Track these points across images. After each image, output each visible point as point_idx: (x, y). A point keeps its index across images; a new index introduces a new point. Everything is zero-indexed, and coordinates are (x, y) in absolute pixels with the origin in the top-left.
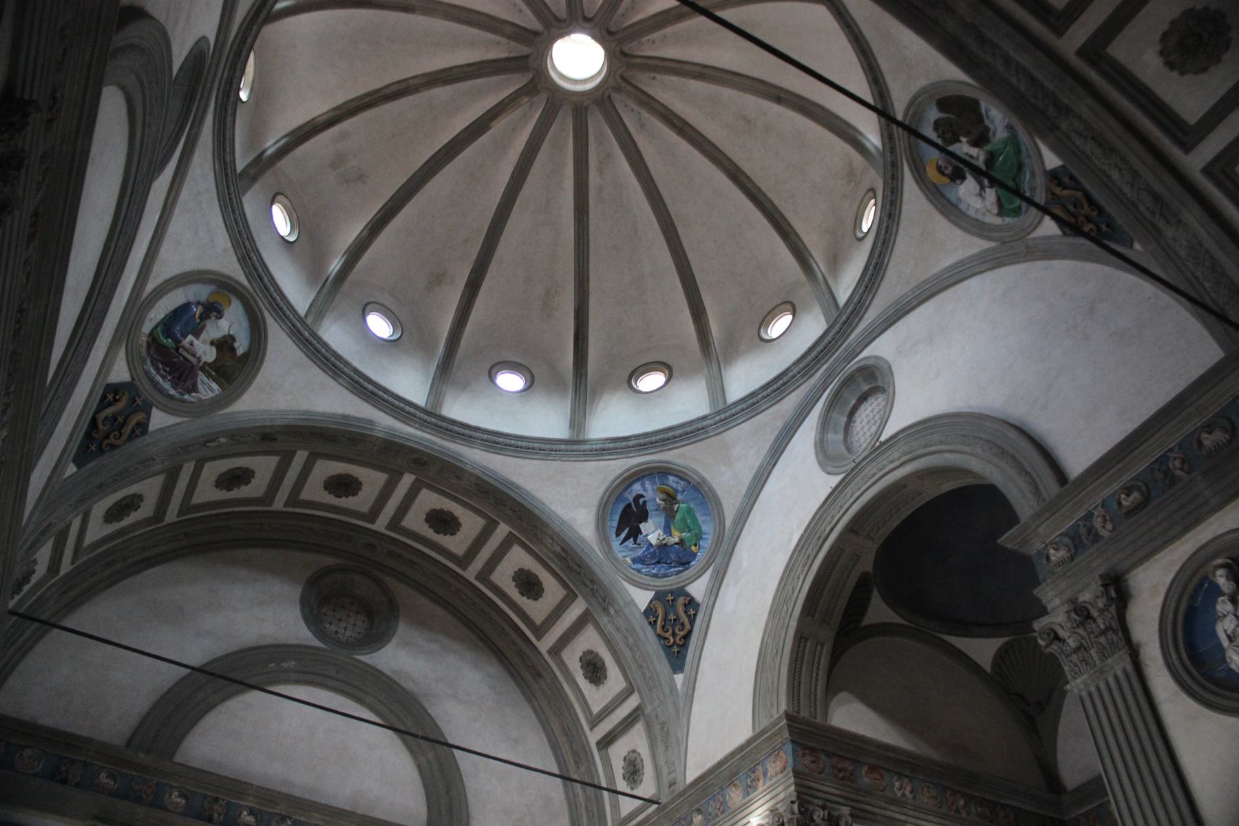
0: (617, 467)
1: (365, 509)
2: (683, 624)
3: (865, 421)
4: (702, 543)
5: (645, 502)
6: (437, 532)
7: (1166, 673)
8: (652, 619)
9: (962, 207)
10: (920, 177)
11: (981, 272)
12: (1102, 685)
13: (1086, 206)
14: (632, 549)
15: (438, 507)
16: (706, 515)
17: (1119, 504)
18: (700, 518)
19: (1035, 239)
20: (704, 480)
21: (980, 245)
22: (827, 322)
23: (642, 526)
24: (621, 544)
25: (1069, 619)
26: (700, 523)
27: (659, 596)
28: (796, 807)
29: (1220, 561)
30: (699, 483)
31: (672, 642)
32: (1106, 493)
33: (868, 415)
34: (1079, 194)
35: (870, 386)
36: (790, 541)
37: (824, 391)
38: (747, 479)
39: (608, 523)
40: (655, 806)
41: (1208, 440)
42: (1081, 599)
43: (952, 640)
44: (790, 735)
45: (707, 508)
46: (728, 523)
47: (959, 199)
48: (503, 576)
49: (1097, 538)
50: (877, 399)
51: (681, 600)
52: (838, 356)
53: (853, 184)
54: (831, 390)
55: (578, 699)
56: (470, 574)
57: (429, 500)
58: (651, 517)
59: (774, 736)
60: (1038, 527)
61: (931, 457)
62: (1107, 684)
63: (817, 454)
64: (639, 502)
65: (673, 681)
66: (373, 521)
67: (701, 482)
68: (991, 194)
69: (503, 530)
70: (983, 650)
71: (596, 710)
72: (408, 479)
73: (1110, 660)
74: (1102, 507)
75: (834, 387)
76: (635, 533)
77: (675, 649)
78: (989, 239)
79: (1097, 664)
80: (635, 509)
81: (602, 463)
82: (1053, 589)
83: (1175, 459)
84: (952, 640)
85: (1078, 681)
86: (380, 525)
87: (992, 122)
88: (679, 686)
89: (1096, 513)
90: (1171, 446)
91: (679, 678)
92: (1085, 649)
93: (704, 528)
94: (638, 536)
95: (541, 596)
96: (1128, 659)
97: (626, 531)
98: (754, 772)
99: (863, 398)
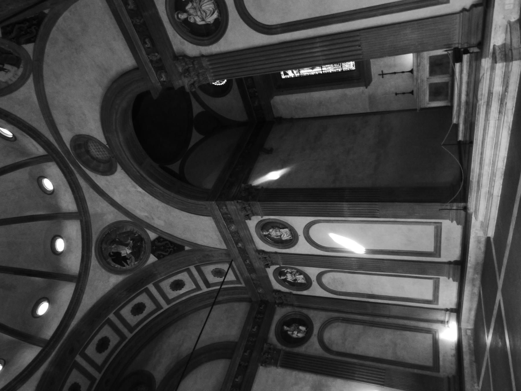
0: (94, 262)
1: (88, 382)
2: (166, 244)
3: (97, 153)
4: (135, 232)
5: (113, 252)
6: (107, 348)
7: (211, 46)
8: (162, 256)
9: (10, 82)
11: (43, 86)
12: (211, 71)
13: (22, 25)
14: (132, 261)
15: (95, 346)
17: (149, 48)
18: (124, 231)
19: (33, 55)
20: (109, 226)
21: (30, 81)
22: (52, 161)
23: (122, 256)
24: (128, 265)
25: (187, 77)
26: (126, 231)
27: (153, 252)
28: (240, 201)
29: (176, 16)
31: (172, 249)
32: (144, 53)
33: (96, 151)
36: (140, 192)
37: (80, 167)
38: (111, 209)
39: (119, 269)
40: (233, 263)
42: (181, 71)
43: (190, 146)
44: (214, 201)
46: (128, 219)
47: (6, 82)
48: (133, 320)
49: (160, 60)
50: (89, 146)
51: (156, 243)
55: (189, 294)
56: (129, 335)
57: (91, 350)
58: (120, 251)
62: (212, 69)
63: (107, 175)
64: (112, 255)
65: (188, 251)
66: (95, 379)
68: (7, 66)
69: (112, 316)
70: (196, 137)
71: (194, 287)
72: (79, 359)
73: (204, 65)
74: (149, 55)
76: (125, 259)
79: (204, 70)
80: (114, 257)
81: (91, 268)
83: (136, 21)
84: (190, 146)
85: (209, 79)
86: (98, 376)
88: (190, 249)
89: (151, 58)
90: (131, 22)
91: (187, 248)
92: (199, 74)
93: (129, 229)
94: (126, 258)
95: (144, 304)
96: (204, 58)
97: (123, 262)
99: (88, 152)
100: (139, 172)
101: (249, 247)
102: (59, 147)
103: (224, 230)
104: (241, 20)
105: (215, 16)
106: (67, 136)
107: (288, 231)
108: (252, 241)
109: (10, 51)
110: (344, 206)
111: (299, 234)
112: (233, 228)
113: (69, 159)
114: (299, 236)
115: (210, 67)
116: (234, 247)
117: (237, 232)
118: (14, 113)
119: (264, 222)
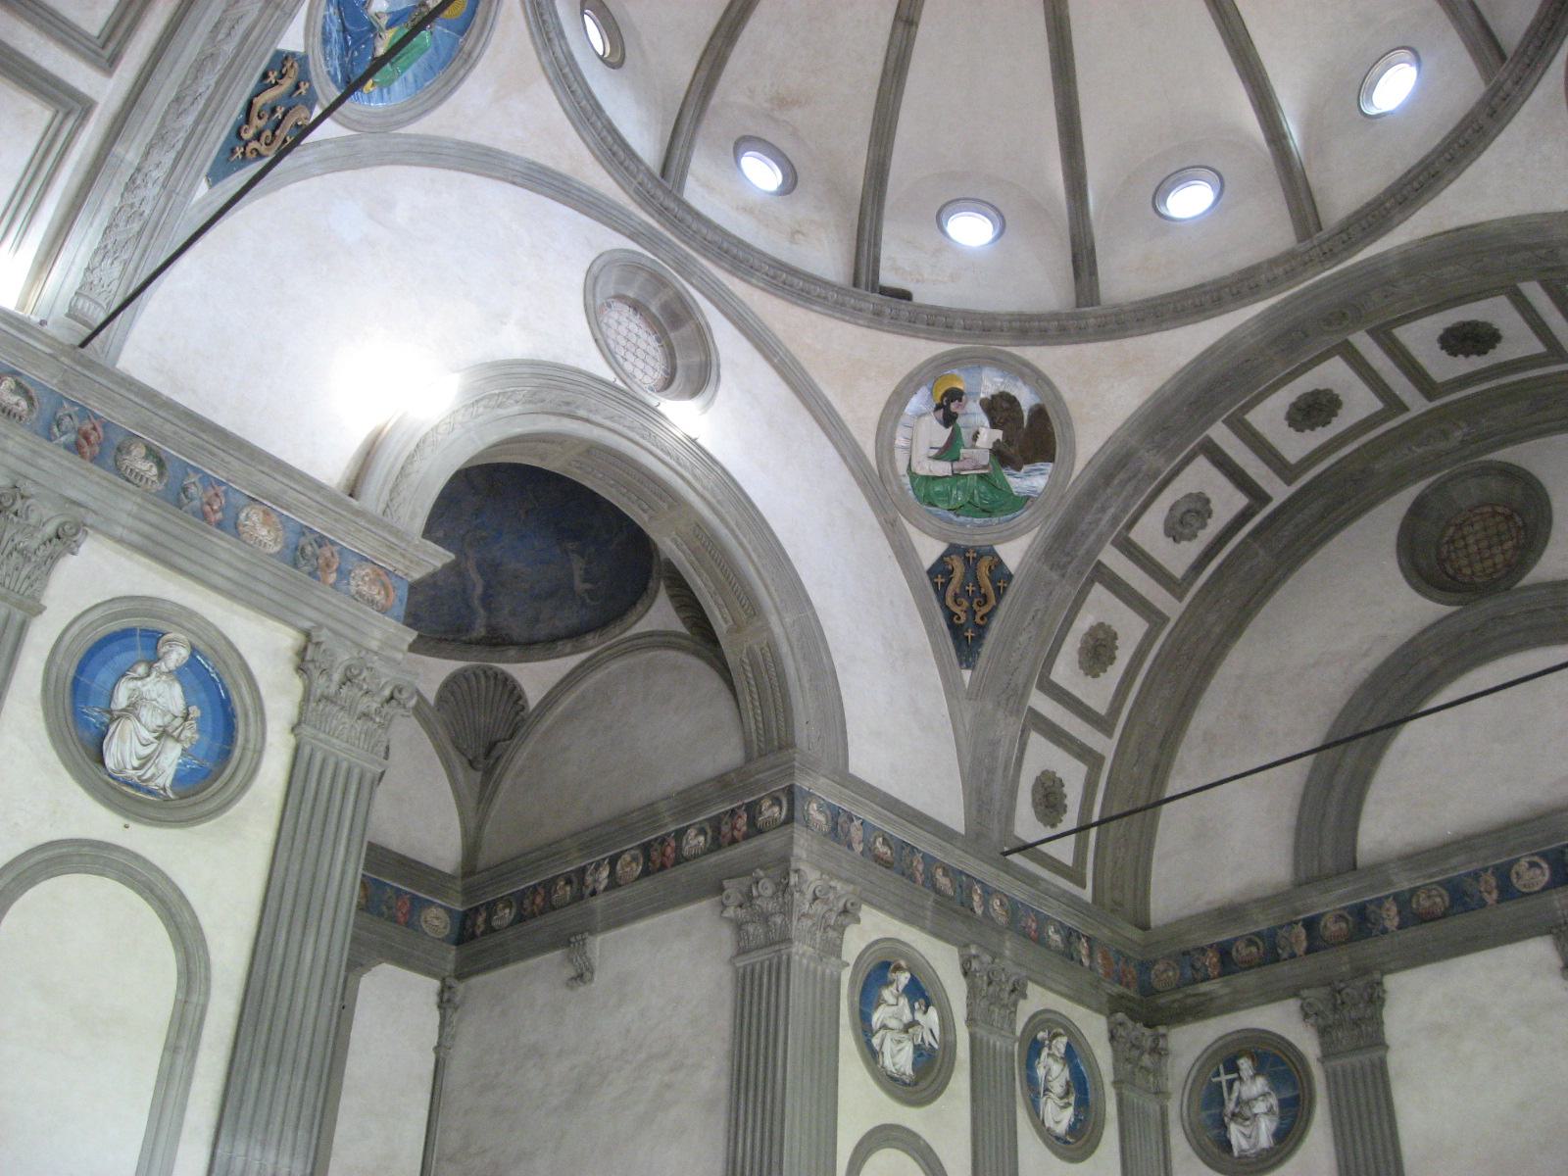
10: (938, 366)
12: (812, 965)
16: (415, 76)
17: (875, 842)
21: (869, 450)
30: (470, 54)
34: (993, 602)
35: (658, 315)
38: (480, 135)
41: (943, 881)
45: (426, 81)
49: (850, 846)
52: (674, 244)
53: (766, 105)
54: (639, 254)
59: (401, 554)
60: (824, 776)
61: (734, 541)
62: (815, 969)
67: (471, 61)
68: (943, 468)
75: (643, 256)
77: (239, 151)
78: (879, 462)
82: (807, 840)
85: (805, 947)
87: (1028, 474)
93: (396, 86)
98: (320, 546)
99: (637, 307)
100: (587, 421)
101: (126, 507)
102: (712, 274)
103: (273, 486)
104: (878, 1124)
105: (888, 1062)
106: (725, 337)
107: (160, 781)
108: (154, 550)
109: (958, 516)
110: (285, 1161)
111: (132, 825)
112: (264, 534)
113: (668, 242)
114: (122, 821)
115: (819, 968)
116: (145, 428)
117: (231, 526)
118: (864, 330)
119: (241, 700)
